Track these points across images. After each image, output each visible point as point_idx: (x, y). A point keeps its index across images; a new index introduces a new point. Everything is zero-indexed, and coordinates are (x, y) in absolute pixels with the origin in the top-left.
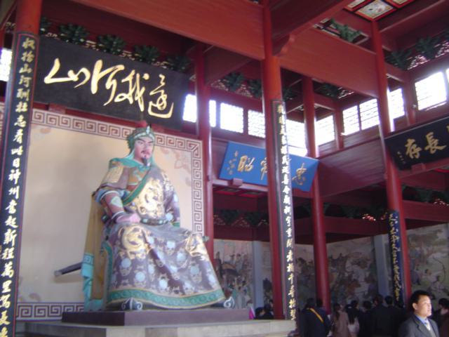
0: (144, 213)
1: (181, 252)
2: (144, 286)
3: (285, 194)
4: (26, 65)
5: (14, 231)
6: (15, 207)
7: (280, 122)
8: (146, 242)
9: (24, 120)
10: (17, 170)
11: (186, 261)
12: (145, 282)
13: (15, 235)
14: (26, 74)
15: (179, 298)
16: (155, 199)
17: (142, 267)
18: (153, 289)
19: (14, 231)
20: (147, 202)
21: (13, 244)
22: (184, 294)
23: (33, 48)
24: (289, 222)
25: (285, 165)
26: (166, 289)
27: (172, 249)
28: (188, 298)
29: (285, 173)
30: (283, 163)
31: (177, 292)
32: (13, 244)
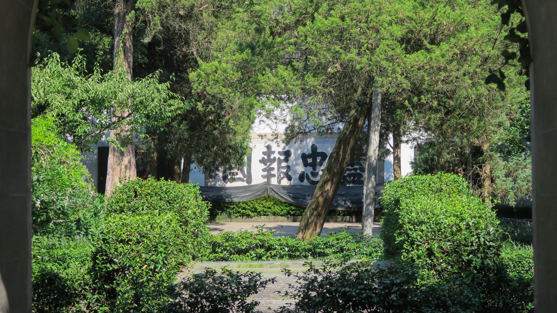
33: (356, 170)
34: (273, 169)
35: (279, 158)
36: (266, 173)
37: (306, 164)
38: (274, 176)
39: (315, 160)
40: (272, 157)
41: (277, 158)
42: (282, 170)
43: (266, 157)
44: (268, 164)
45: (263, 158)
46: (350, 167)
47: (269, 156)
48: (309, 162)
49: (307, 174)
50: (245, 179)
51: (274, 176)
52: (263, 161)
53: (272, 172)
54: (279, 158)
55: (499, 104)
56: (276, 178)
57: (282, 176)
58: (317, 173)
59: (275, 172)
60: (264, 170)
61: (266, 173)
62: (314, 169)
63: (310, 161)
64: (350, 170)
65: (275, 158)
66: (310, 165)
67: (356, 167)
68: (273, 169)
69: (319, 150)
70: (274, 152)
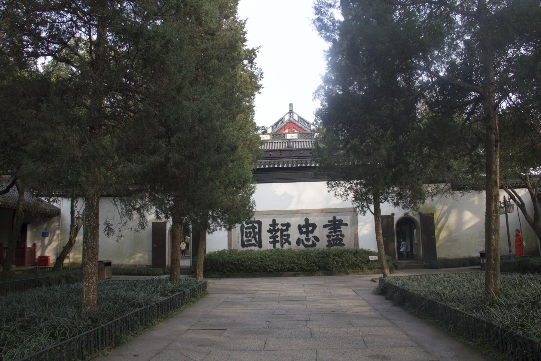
33: (337, 235)
34: (277, 237)
35: (281, 228)
36: (272, 240)
37: (301, 232)
38: (278, 241)
39: (307, 229)
41: (280, 229)
42: (284, 237)
43: (272, 228)
44: (274, 233)
46: (333, 234)
48: (303, 231)
49: (302, 240)
50: (257, 244)
51: (278, 241)
53: (277, 239)
54: (281, 228)
56: (280, 243)
58: (310, 239)
59: (279, 239)
60: (271, 238)
62: (307, 236)
63: (304, 230)
64: (333, 236)
65: (278, 228)
66: (304, 233)
67: (337, 233)
68: (277, 237)
69: (310, 222)
70: (278, 224)
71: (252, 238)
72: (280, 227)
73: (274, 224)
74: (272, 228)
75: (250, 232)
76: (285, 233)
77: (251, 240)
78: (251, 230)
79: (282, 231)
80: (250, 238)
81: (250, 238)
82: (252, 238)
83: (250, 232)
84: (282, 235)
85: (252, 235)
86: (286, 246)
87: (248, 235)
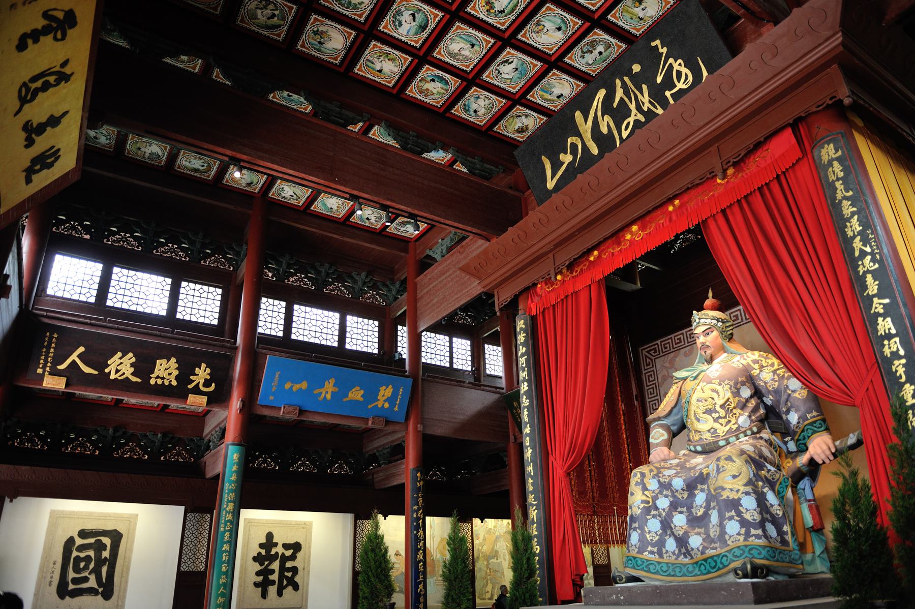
0: (697, 438)
1: (702, 490)
2: (636, 550)
3: (878, 315)
4: (521, 347)
5: (535, 507)
6: (532, 484)
7: (832, 178)
8: (645, 488)
9: (526, 399)
10: (529, 448)
11: (704, 504)
12: (637, 546)
13: (536, 511)
14: (523, 355)
15: (685, 565)
16: (709, 412)
17: (636, 525)
18: (652, 552)
19: (535, 507)
20: (698, 420)
21: (535, 521)
22: (692, 558)
23: (524, 326)
24: (901, 371)
25: (863, 254)
26: (674, 553)
27: (682, 489)
28: (696, 563)
29: (865, 273)
30: (857, 254)
31: (685, 557)
32: (535, 521)
34: (273, 571)
35: (283, 553)
36: (260, 579)
38: (273, 583)
40: (273, 552)
42: (286, 574)
43: (263, 552)
45: (259, 553)
47: (268, 551)
51: (273, 583)
52: (258, 559)
53: (271, 577)
54: (283, 553)
55: (773, 469)
56: (276, 587)
57: (285, 582)
59: (275, 577)
61: (260, 579)
65: (277, 553)
68: (273, 571)
70: (276, 545)
71: (89, 574)
72: (279, 550)
73: (269, 542)
74: (263, 552)
75: (89, 557)
76: (289, 564)
77: (86, 579)
78: (91, 553)
79: (284, 559)
80: (85, 574)
81: (85, 574)
82: (89, 574)
83: (88, 559)
84: (282, 568)
85: (92, 566)
86: (288, 591)
87: (82, 565)
